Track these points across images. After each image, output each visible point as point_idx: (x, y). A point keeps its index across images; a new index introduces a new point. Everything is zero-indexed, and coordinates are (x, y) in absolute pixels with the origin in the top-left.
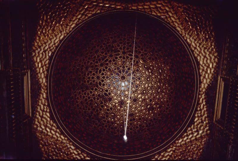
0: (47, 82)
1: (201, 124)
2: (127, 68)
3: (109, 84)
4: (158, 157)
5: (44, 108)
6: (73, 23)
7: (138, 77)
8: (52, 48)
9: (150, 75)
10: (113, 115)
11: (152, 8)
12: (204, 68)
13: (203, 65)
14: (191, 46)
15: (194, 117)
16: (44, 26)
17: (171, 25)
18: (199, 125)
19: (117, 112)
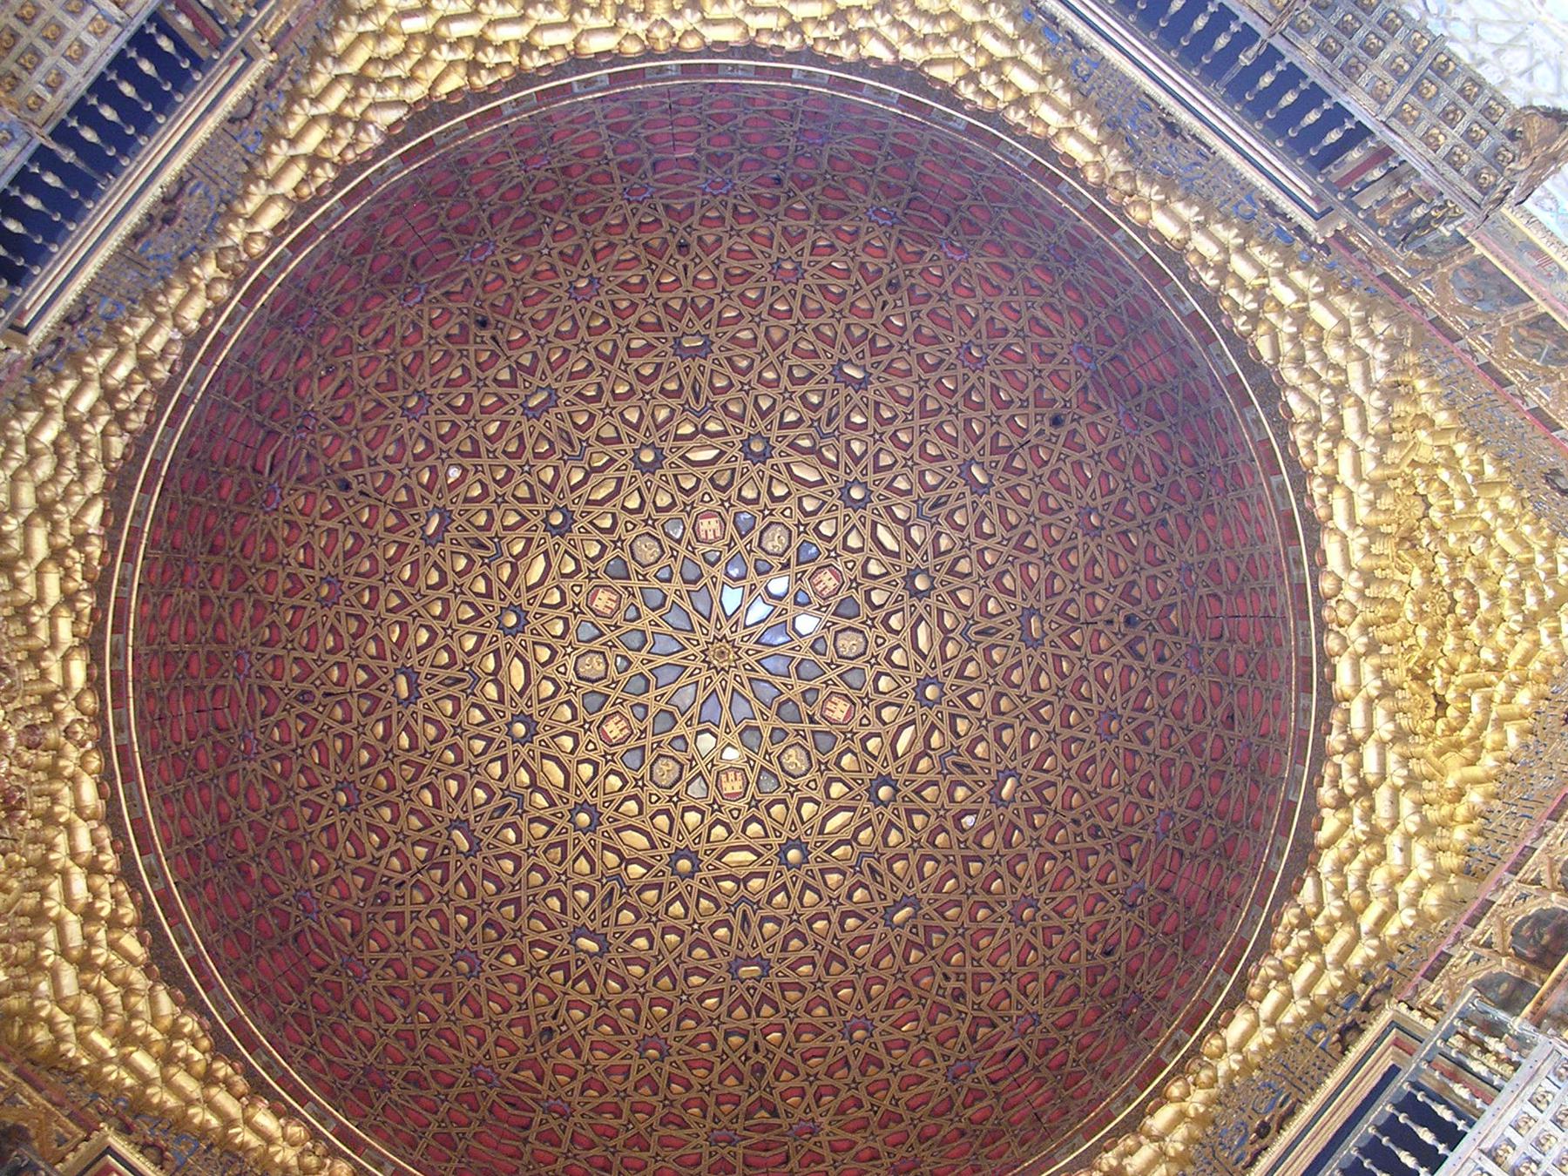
0: (1144, 230)
3: (755, 535)
4: (88, 558)
5: (1004, 84)
6: (1358, 687)
8: (1322, 445)
9: (609, 855)
15: (191, 1003)
16: (1470, 502)
18: (116, 1000)
19: (529, 442)
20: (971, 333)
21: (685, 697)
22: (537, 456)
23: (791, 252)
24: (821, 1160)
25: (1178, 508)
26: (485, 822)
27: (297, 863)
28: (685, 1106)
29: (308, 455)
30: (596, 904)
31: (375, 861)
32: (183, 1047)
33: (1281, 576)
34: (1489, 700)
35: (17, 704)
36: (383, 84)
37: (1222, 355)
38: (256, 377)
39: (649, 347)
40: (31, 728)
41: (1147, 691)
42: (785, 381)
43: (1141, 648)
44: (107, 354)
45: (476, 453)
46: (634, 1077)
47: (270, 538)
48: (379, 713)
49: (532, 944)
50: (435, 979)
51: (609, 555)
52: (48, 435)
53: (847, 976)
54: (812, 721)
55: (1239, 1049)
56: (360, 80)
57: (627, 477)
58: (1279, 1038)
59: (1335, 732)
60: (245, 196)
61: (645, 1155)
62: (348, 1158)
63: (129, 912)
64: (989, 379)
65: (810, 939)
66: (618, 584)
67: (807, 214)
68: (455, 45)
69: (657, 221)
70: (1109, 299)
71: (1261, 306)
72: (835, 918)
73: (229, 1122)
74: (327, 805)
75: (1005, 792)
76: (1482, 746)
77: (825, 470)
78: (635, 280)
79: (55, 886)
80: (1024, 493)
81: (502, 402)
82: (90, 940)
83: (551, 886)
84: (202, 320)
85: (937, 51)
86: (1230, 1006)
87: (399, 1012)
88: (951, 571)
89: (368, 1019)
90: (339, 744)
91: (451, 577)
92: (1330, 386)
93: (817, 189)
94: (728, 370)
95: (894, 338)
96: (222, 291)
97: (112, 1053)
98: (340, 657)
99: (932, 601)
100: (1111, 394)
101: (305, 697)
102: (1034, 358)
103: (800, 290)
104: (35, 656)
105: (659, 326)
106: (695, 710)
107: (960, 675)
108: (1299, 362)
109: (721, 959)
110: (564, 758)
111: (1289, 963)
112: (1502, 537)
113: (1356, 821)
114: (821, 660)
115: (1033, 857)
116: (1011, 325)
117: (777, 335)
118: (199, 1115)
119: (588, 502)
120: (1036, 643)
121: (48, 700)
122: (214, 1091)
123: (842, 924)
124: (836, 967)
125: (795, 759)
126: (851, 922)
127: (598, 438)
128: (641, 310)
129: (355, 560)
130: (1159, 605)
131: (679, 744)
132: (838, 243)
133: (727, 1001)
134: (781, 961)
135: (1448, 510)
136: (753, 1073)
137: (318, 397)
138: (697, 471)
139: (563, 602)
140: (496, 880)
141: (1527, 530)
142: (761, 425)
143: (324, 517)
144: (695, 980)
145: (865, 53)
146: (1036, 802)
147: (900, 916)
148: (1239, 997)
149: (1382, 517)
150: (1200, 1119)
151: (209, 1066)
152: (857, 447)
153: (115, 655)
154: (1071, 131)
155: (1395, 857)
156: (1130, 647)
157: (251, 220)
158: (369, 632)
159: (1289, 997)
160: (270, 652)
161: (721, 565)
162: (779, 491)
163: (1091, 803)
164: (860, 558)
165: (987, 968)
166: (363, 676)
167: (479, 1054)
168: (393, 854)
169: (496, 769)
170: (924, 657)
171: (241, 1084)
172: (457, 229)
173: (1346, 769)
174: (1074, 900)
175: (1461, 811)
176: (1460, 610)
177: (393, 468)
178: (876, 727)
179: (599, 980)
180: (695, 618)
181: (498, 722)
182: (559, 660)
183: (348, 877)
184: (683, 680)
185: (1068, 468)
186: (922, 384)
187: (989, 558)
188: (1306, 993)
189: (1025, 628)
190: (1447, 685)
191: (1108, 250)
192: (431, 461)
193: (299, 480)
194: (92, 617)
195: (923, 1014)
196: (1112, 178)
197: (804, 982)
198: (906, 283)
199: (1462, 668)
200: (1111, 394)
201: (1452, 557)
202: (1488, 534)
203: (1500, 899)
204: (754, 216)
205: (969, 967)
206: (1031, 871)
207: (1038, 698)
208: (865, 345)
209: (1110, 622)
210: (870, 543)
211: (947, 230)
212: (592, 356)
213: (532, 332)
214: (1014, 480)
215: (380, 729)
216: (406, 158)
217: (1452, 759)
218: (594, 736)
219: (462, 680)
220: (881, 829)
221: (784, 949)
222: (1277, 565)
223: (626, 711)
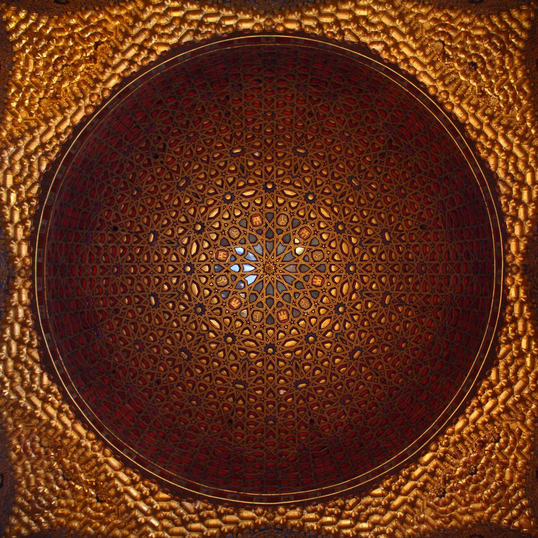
0: (31, 255)
1: (518, 362)
2: (282, 235)
3: (226, 288)
4: (391, 482)
5: (23, 334)
6: (112, 76)
7: (318, 264)
8: (49, 148)
10: (241, 386)
11: (342, 20)
12: (511, 189)
13: (508, 181)
14: (468, 127)
15: (497, 344)
16: (28, 87)
17: (401, 71)
19: (254, 378)
20: (111, 276)
21: (291, 268)
23: (132, 350)
24: (392, 116)
25: (110, 172)
26: (377, 297)
27: (433, 343)
28: (410, 169)
29: (312, 440)
30: (374, 244)
31: (414, 320)
32: (511, 335)
33: (101, 125)
34: (84, 31)
35: (451, 467)
36: (180, 515)
37: (49, 200)
38: (300, 476)
39: (197, 367)
40: (455, 457)
41: (173, 134)
42: (173, 318)
43: (161, 147)
44: (327, 528)
45: (271, 391)
46: (414, 191)
47: (345, 431)
48: (371, 355)
49: (400, 253)
50: (434, 274)
51: (268, 326)
52: (365, 525)
53: (332, 152)
54: (266, 225)
55: (251, 20)
57: (240, 341)
58: (238, 10)
60: (247, 527)
61: (434, 170)
62: (505, 259)
63: (485, 384)
64: (120, 259)
65: (331, 173)
66: (274, 316)
67: (117, 355)
68: (150, 504)
69: (157, 396)
70: (64, 246)
71: (23, 202)
72: (319, 170)
73: (522, 304)
74: (409, 348)
75: (238, 151)
76: (98, 22)
77: (189, 284)
78: (180, 388)
79: (494, 412)
80: (145, 220)
81: (249, 396)
82: (502, 389)
83: (379, 262)
84: (294, 508)
85: (30, 362)
87: (452, 277)
88: (187, 221)
89: (461, 285)
90: (389, 359)
91: (313, 367)
92: (29, 160)
93: (106, 359)
94: (184, 338)
95: (132, 297)
96: (281, 509)
97: (529, 355)
98: (363, 380)
99: (201, 220)
100: (93, 220)
101: (383, 381)
102: (102, 252)
103: (142, 337)
104: (433, 474)
105: (188, 369)
106: (292, 262)
107: (216, 193)
108: (30, 176)
109: (359, 194)
110: (339, 289)
111: (213, 26)
112: (31, 69)
113: (153, 42)
114: (246, 238)
115: (251, 127)
116: (98, 267)
117: (161, 333)
118: (527, 314)
119: (257, 345)
120: (188, 180)
121: (442, 459)
122: (516, 315)
123: (319, 167)
124: (333, 158)
125: (282, 221)
126: (316, 164)
127: (236, 358)
128: (187, 379)
129: (331, 400)
130: (143, 153)
131: (306, 259)
132: (117, 337)
133: (370, 182)
134: (345, 176)
135: (37, 92)
136: (384, 157)
137: (292, 452)
138: (221, 321)
139: (293, 328)
140: (391, 280)
141: (22, 63)
142: (192, 314)
143: (325, 419)
144: (371, 196)
145: (50, 383)
146: (234, 139)
147: (302, 151)
149: (56, 111)
150: (283, 15)
151: (511, 323)
152: (174, 281)
153: (414, 450)
154: (20, 301)
155: (154, 22)
156: (164, 150)
157: (253, 519)
158: (349, 378)
159: (225, 18)
160: (378, 403)
161: (243, 290)
162: (207, 292)
163: (220, 123)
164: (206, 252)
165: (295, 113)
166: (363, 369)
167: (445, 243)
168: (408, 316)
169: (358, 306)
171: (509, 308)
172: (208, 453)
174: (253, 104)
175: (123, 12)
176: (64, 62)
177: (295, 411)
178: (252, 205)
179: (395, 225)
180: (265, 285)
181: (344, 317)
182: (311, 315)
183: (425, 324)
184: (287, 273)
185: (127, 213)
186: (139, 277)
187: (174, 214)
188: (217, 14)
189: (185, 186)
190: (90, 48)
191: (49, 260)
192: (284, 402)
193: (321, 436)
194: (408, 467)
195: (325, 120)
196: (24, 277)
197: (345, 163)
198: (113, 308)
199: (81, 47)
200: (93, 220)
201: (50, 79)
202: (33, 74)
204: (131, 370)
205: (300, 118)
206: (256, 124)
207: (203, 165)
208: (142, 304)
209: (162, 162)
210: (200, 252)
211: (86, 310)
212: (213, 381)
213: (221, 405)
214: (144, 226)
215: (375, 351)
216: (198, 489)
217: (110, 28)
218: (325, 286)
219: (340, 338)
220: (281, 178)
221: (340, 177)
222: (99, 128)
223: (310, 282)
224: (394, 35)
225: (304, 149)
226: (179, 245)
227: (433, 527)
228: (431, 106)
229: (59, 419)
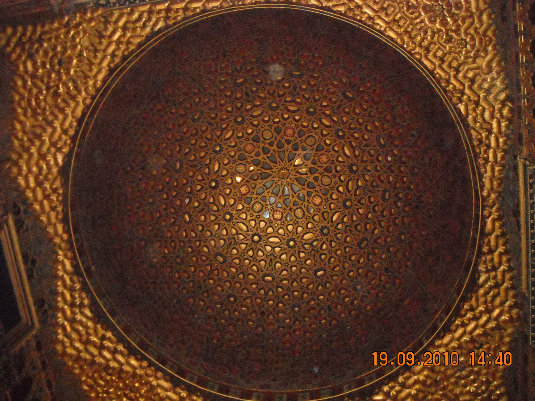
3: (305, 209)
7: (275, 134)
11: (43, 193)
13: (151, 23)
19: (379, 183)
22: (374, 180)
33: (173, 355)
36: (491, 288)
56: (497, 286)
59: (122, 348)
66: (325, 166)
75: (187, 216)
86: (75, 266)
111: (74, 293)
115: (163, 212)
138: (333, 211)
148: (77, 271)
155: (77, 345)
170: (237, 223)
173: (110, 345)
189: (222, 256)
203: (43, 374)
210: (277, 235)
218: (293, 126)
224: (44, 149)
225: (175, 164)
226: (272, 255)
227: (495, 56)
228: (103, 95)
229: (410, 387)
